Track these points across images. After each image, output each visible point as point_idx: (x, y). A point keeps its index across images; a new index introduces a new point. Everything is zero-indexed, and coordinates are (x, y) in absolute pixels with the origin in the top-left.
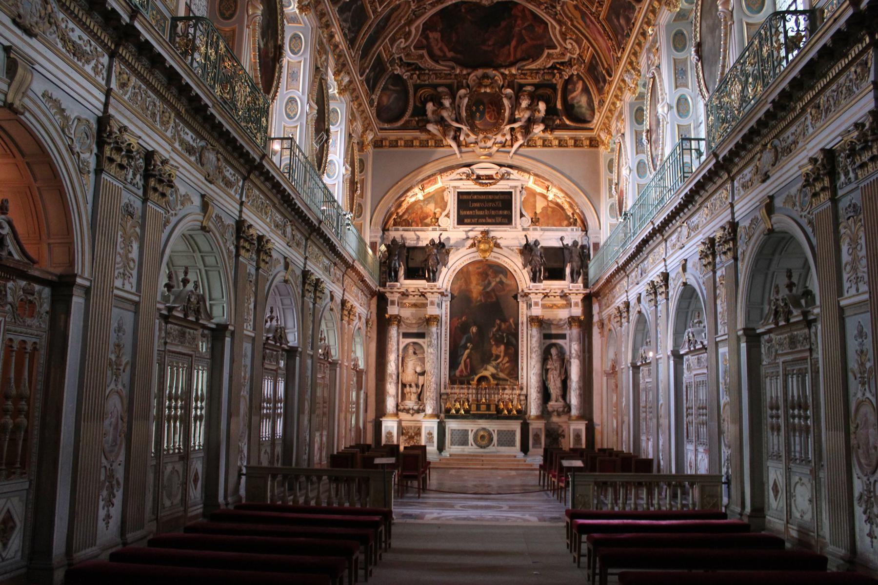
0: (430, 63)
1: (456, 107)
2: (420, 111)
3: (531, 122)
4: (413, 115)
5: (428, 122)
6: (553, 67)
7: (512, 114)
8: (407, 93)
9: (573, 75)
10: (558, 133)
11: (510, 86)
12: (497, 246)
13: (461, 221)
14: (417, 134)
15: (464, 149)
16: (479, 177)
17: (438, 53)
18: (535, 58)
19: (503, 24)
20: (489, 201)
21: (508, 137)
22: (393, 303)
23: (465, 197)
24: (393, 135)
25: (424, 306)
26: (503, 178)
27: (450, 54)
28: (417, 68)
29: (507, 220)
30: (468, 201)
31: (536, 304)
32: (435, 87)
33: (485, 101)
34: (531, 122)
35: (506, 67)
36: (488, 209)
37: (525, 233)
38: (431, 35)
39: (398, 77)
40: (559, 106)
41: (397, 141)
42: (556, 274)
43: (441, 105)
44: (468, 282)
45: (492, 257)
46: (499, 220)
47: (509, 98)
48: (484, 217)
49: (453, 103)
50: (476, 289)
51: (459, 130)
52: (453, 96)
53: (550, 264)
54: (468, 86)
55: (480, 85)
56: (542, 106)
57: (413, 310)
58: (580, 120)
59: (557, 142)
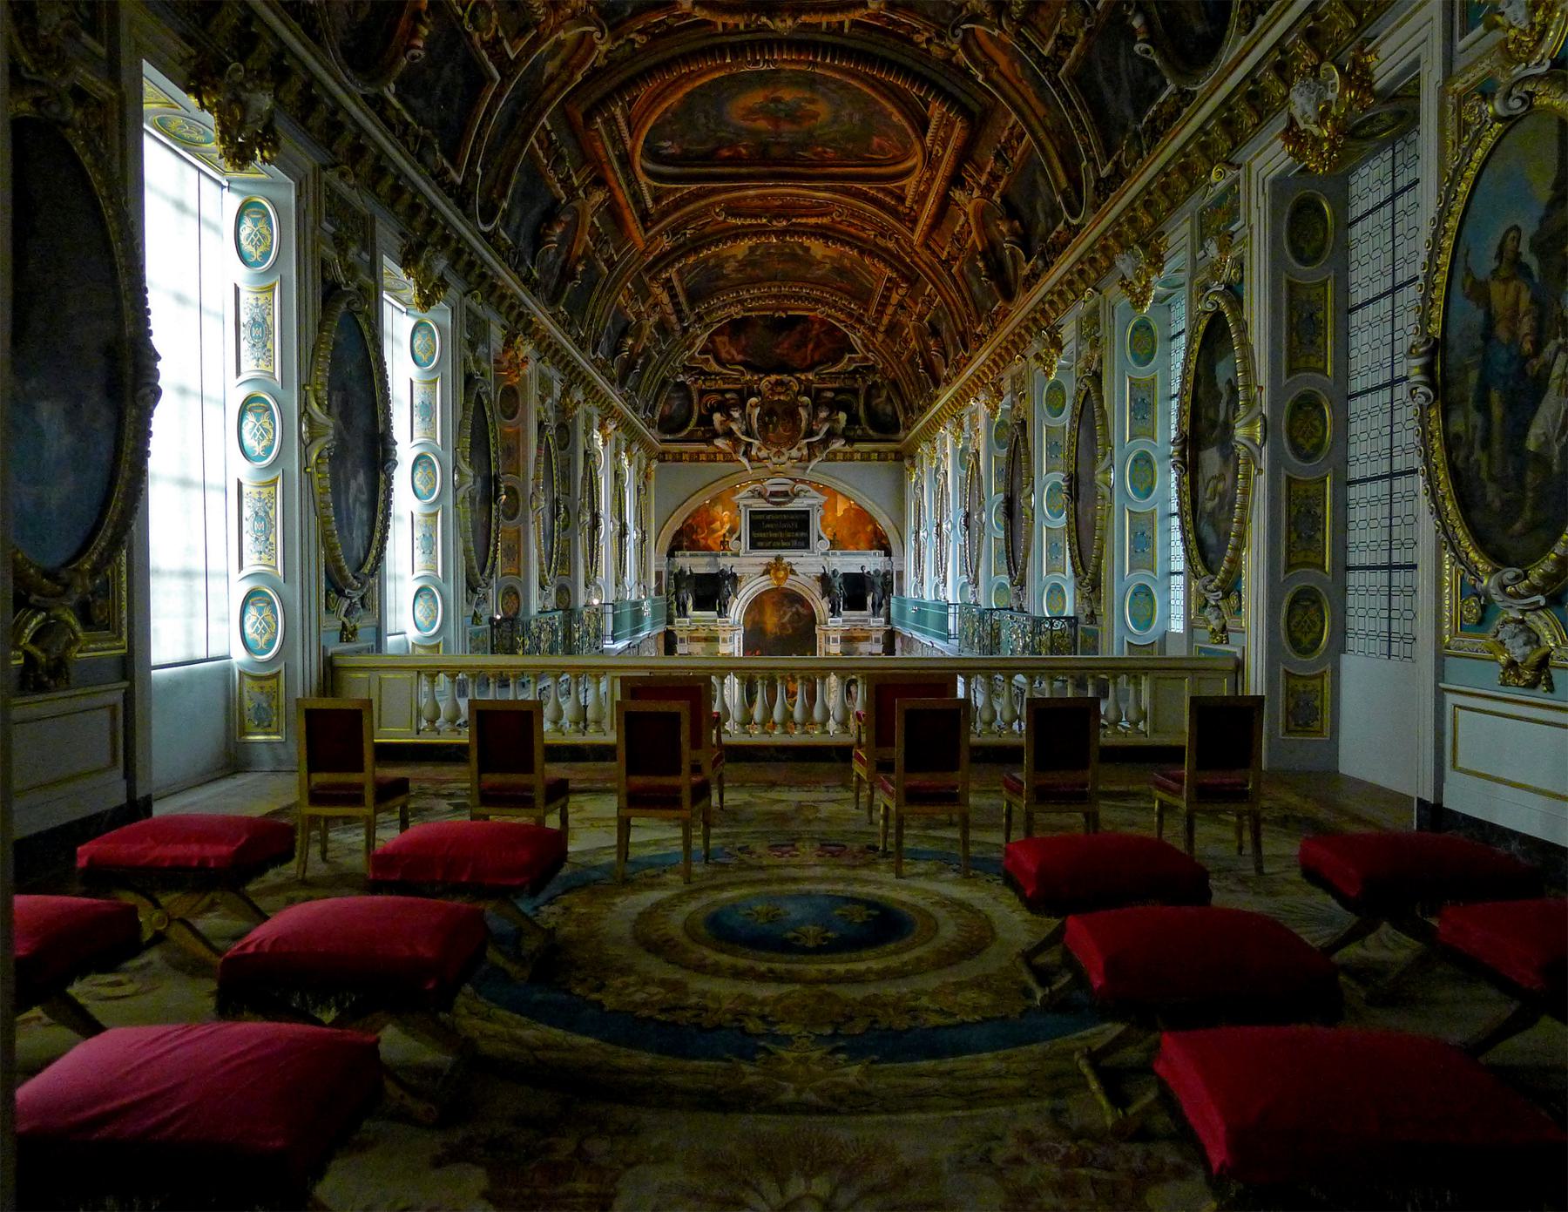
0: (717, 368)
1: (746, 417)
2: (706, 420)
3: (831, 435)
4: (698, 424)
5: (716, 435)
6: (856, 371)
7: (809, 424)
8: (691, 400)
9: (875, 383)
10: (857, 446)
11: (807, 393)
12: (793, 572)
13: (754, 545)
14: (703, 447)
15: (756, 464)
16: (774, 494)
17: (724, 355)
18: (836, 361)
19: (799, 328)
20: (784, 521)
21: (805, 452)
22: (682, 640)
23: (760, 517)
24: (676, 447)
25: (716, 639)
26: (797, 495)
27: (739, 358)
28: (702, 372)
29: (805, 544)
30: (759, 521)
31: (835, 640)
32: (722, 392)
33: (779, 411)
34: (831, 435)
35: (803, 371)
36: (783, 530)
37: (821, 559)
38: (718, 339)
39: (683, 383)
40: (861, 413)
41: (681, 454)
42: (856, 603)
43: (730, 417)
44: (761, 612)
45: (786, 585)
46: (795, 543)
47: (805, 406)
48: (777, 539)
49: (743, 415)
50: (771, 621)
51: (750, 444)
52: (743, 408)
53: (853, 592)
54: (759, 393)
55: (774, 393)
56: (842, 417)
57: (703, 644)
58: (886, 427)
59: (857, 456)
